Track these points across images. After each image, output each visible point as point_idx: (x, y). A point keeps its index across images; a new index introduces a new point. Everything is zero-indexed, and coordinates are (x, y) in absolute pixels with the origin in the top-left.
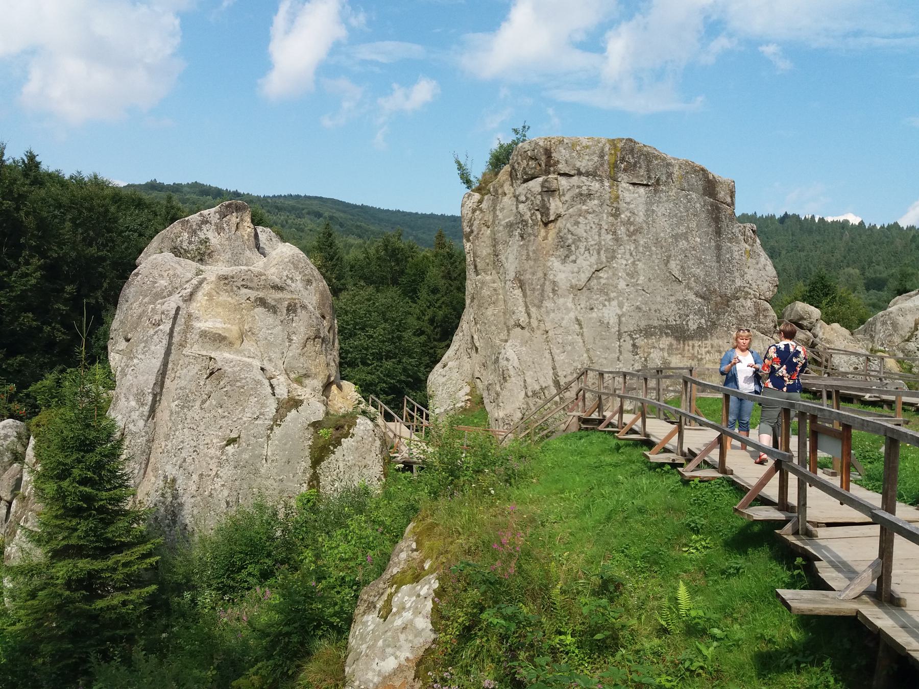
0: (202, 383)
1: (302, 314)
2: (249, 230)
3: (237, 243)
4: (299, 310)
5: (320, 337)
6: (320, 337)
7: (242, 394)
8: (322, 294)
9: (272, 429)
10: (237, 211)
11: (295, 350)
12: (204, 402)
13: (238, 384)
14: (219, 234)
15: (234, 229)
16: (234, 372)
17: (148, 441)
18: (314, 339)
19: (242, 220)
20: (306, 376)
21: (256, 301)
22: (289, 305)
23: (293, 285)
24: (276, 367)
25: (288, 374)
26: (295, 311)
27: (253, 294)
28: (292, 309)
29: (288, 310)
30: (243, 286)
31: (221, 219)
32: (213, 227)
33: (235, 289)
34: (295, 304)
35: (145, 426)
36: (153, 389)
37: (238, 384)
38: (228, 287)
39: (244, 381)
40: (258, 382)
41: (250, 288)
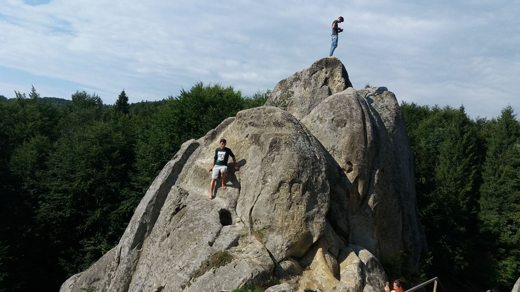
0: (169, 218)
1: (286, 152)
2: (339, 84)
3: (320, 96)
4: (283, 148)
5: (300, 182)
6: (300, 182)
7: (189, 237)
8: (353, 137)
9: (183, 287)
10: (326, 67)
11: (265, 195)
12: (163, 240)
13: (191, 225)
14: (305, 89)
15: (321, 84)
16: (193, 211)
17: (128, 269)
18: (291, 183)
19: (332, 75)
20: (270, 228)
21: (252, 138)
22: (274, 142)
23: (321, 126)
24: (242, 213)
25: (251, 223)
26: (278, 149)
27: (251, 130)
28: (275, 145)
29: (271, 146)
30: (250, 123)
31: (311, 76)
32: (302, 83)
33: (244, 126)
34: (281, 140)
35: (129, 253)
36: (142, 218)
37: (191, 225)
38: (240, 126)
39: (197, 223)
40: (207, 225)
41: (256, 126)
